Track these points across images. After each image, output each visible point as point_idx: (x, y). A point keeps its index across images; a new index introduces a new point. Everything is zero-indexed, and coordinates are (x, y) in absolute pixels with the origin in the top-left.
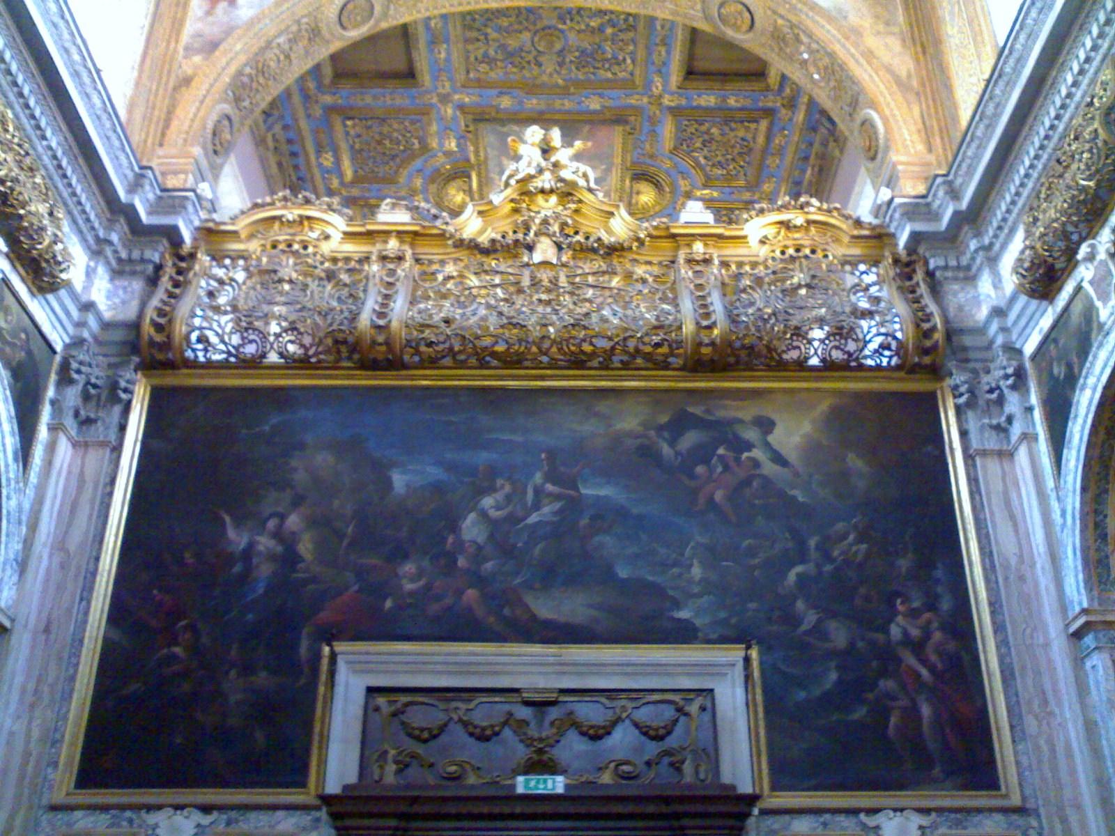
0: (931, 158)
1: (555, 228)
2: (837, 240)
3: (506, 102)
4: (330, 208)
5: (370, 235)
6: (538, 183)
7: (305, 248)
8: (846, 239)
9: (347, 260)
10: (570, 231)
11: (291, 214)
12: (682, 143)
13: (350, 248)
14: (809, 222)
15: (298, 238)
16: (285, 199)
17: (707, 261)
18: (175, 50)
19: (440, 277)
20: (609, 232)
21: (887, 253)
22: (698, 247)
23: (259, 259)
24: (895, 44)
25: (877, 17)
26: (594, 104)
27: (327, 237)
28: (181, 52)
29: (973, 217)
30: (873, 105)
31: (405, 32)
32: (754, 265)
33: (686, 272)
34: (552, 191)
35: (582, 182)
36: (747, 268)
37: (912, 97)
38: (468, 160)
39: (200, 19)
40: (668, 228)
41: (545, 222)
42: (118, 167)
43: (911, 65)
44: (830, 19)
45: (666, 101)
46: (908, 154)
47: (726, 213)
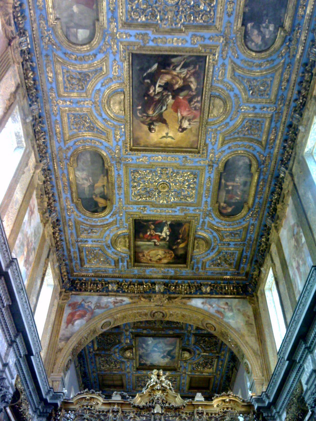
0: (264, 378)
1: (160, 401)
2: (238, 406)
3: (145, 332)
4: (99, 395)
5: (110, 404)
6: (156, 387)
7: (91, 407)
8: (241, 406)
9: (103, 411)
10: (164, 402)
11: (88, 397)
12: (197, 342)
13: (105, 408)
14: (230, 400)
15: (90, 404)
16: (87, 392)
17: (202, 413)
18: (57, 341)
19: (129, 418)
20: (175, 402)
21: (252, 411)
22: (200, 408)
23: (79, 411)
24: (253, 339)
25: (249, 331)
26: (171, 332)
27: (98, 404)
28: (59, 340)
29: (274, 403)
30: (248, 360)
31: (118, 327)
32: (215, 414)
33: (197, 417)
34: (160, 389)
35: (168, 388)
36: (213, 415)
37: (258, 357)
38: (132, 345)
39: (64, 330)
40: (192, 402)
41: (158, 399)
42: (44, 388)
43: (258, 347)
44: (236, 332)
45: (192, 332)
46: (257, 376)
47: (209, 398)
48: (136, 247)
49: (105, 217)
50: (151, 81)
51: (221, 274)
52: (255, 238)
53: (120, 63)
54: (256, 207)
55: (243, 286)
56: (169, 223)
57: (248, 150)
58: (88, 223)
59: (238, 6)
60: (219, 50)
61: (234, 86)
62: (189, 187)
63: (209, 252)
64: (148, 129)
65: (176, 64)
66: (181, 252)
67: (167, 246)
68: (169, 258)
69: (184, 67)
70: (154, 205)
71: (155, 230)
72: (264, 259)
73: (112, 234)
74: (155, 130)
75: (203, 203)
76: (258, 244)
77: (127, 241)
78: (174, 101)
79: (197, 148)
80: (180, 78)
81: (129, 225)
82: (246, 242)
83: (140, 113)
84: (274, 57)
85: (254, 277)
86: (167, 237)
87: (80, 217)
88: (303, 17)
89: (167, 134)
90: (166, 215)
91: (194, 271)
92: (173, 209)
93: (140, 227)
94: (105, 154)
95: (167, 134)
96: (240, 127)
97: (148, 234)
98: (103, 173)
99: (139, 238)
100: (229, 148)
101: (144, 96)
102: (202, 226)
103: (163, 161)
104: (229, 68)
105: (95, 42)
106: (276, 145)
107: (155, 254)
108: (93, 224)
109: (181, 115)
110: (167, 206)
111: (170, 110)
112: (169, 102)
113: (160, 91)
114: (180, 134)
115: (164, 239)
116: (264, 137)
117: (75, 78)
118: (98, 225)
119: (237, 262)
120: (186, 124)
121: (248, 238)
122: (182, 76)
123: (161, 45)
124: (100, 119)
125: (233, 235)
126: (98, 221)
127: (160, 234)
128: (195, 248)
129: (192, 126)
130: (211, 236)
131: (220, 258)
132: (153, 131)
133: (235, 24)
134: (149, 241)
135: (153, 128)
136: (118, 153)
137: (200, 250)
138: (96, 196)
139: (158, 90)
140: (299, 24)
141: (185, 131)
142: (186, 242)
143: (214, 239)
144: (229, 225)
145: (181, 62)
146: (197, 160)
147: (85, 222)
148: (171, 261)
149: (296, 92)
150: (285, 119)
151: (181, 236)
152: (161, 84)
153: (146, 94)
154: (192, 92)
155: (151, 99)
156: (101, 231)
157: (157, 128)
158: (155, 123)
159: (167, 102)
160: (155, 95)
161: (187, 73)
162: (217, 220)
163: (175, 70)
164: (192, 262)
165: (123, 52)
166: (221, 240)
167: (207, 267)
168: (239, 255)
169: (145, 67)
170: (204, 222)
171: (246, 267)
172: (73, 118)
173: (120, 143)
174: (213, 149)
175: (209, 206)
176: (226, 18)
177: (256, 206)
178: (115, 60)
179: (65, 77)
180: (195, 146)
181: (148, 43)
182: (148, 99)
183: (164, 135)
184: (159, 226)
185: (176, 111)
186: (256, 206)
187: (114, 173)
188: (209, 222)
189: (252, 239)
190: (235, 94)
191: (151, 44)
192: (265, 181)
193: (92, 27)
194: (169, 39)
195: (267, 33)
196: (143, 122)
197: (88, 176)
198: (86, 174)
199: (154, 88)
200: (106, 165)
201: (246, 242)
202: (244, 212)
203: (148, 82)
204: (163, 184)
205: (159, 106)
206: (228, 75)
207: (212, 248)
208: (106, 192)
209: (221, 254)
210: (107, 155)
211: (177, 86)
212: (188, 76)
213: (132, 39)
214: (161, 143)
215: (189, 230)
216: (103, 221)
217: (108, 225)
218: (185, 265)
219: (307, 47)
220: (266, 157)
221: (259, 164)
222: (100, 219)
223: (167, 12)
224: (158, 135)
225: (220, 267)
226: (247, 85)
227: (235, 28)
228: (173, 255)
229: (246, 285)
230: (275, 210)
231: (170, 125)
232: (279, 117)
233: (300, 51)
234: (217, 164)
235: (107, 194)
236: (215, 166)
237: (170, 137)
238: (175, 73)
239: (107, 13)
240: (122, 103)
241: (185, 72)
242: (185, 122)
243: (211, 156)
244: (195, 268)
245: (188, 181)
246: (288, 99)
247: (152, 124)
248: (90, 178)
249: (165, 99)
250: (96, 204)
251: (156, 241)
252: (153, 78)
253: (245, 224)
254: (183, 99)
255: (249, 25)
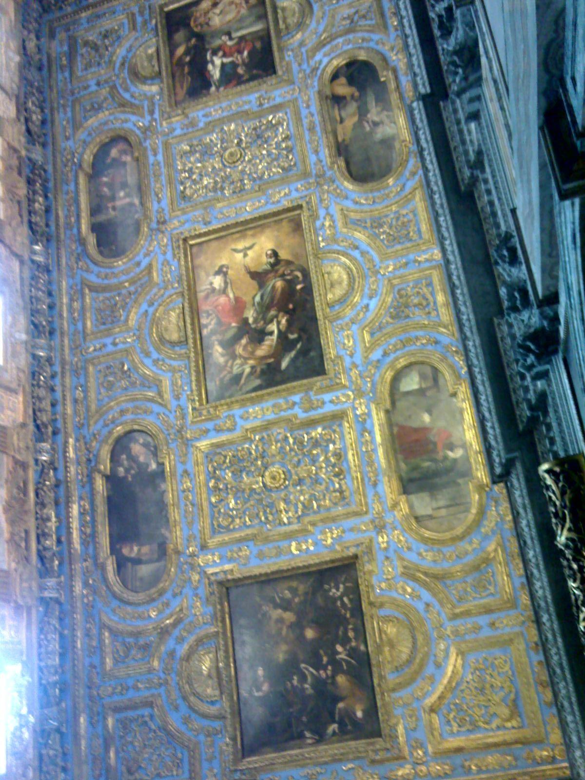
48: (263, 17)
49: (330, 60)
50: (287, 338)
51: (98, 17)
52: (56, 112)
53: (342, 353)
54: (70, 175)
55: (49, 7)
56: (213, 89)
57: (108, 271)
58: (360, 35)
59: (175, 488)
60: (190, 418)
61: (154, 369)
62: (191, 171)
63: (130, 55)
64: (280, 254)
65: (252, 377)
66: (180, 36)
67: (208, 39)
68: (198, 14)
69: (241, 374)
70: (245, 115)
71: (234, 65)
72: (23, 78)
73: (313, 25)
74: (267, 255)
75: (161, 150)
76: (47, 105)
77: (281, 22)
78: (245, 316)
79: (191, 246)
80: (241, 356)
81: (282, 59)
82: (71, 99)
83: (298, 277)
84: (105, 431)
85: (33, 36)
86: (211, 58)
87: (377, 43)
88: (81, 498)
89: (245, 255)
90: (220, 102)
91: (147, 4)
92: (210, 119)
93: (262, 62)
94: (346, 184)
95: (245, 255)
96: (129, 306)
97: (246, 53)
98: (347, 146)
99: (261, 38)
100: (138, 264)
101: (294, 310)
102: (153, 104)
103: (243, 205)
104: (167, 396)
105: (389, 375)
106: (68, 293)
107: (227, 13)
108: (351, 36)
109: (228, 296)
110: (222, 121)
111: (247, 299)
112: (252, 312)
113: (270, 326)
114: (224, 262)
115: (215, 53)
116: (88, 301)
117: (415, 306)
118: (341, 36)
119: (76, 52)
120: (218, 282)
121: (69, 109)
122: (238, 361)
123: (281, 401)
124: (364, 247)
125: (96, 106)
126: (343, 44)
127: (226, 60)
128: (155, 54)
129: (208, 282)
130: (133, 89)
131: (107, 50)
132: (269, 252)
133: (173, 463)
134: (242, 39)
135: (271, 257)
136: (323, 193)
137: (146, 52)
138: (352, 96)
139: (273, 327)
140: (83, 487)
141: (217, 269)
142: (174, 61)
143: (127, 84)
144: (106, 123)
145: (244, 384)
146: (187, 226)
147: (366, 35)
148: (194, 9)
149: (59, 389)
150: (62, 341)
151: (186, 69)
152: (270, 337)
153: (290, 313)
154: (217, 340)
155: (282, 308)
156: (333, 26)
157: (265, 259)
158: (268, 267)
159: (255, 310)
160: (277, 316)
161: (232, 367)
162: (129, 125)
163: (253, 367)
164: (154, 22)
165: (340, 373)
166: (114, 87)
167: (126, 21)
168: (75, 69)
169: (301, 359)
170: (152, 113)
171: (58, 47)
172: (411, 234)
173: (322, 213)
174: (165, 253)
175: (149, 147)
176: (190, 467)
177: (71, 176)
178: (351, 356)
179: (432, 304)
180: (195, 250)
181: (301, 399)
182: (287, 305)
183: (250, 253)
184: (230, 77)
185: (237, 299)
186: (71, 176)
187: (325, 153)
188: (143, 116)
189: (61, 110)
190: (150, 357)
191: (296, 398)
192: (69, 226)
193: (397, 397)
194: (269, 413)
195: (125, 463)
196: (289, 263)
197: (371, 133)
198: (376, 133)
199: (281, 327)
200: (342, 164)
201: (71, 99)
202: (88, 157)
203: (292, 333)
204: (234, 162)
205: (267, 299)
206: (166, 384)
207: (127, 65)
208: (336, 111)
209: (106, 59)
210: (342, 184)
211: (244, 341)
212: (229, 364)
213: (327, 397)
214: (253, 236)
215: (174, 87)
216: (332, 50)
217: (321, 45)
218: (166, 9)
219: (61, 458)
220: (78, 268)
221: (85, 252)
222: (339, 52)
223: (279, 453)
224: (258, 249)
225: (103, 30)
226: (134, 376)
227: (172, 457)
228: (192, 24)
229: (45, 11)
230: (30, 182)
231: (243, 271)
232: (74, 341)
233: (71, 450)
234: (151, 230)
235: (333, 107)
236: (154, 225)
237: (240, 251)
238: (251, 362)
239: (373, 426)
240: (328, 286)
241: (235, 368)
242: (220, 286)
243: (165, 240)
244: (147, 12)
245: (195, 182)
246: (68, 374)
247: (273, 265)
248: (368, 129)
249: (258, 314)
250: (351, 81)
251: (230, 43)
252: (284, 344)
253: (81, 135)
254: (230, 324)
255: (154, 466)
